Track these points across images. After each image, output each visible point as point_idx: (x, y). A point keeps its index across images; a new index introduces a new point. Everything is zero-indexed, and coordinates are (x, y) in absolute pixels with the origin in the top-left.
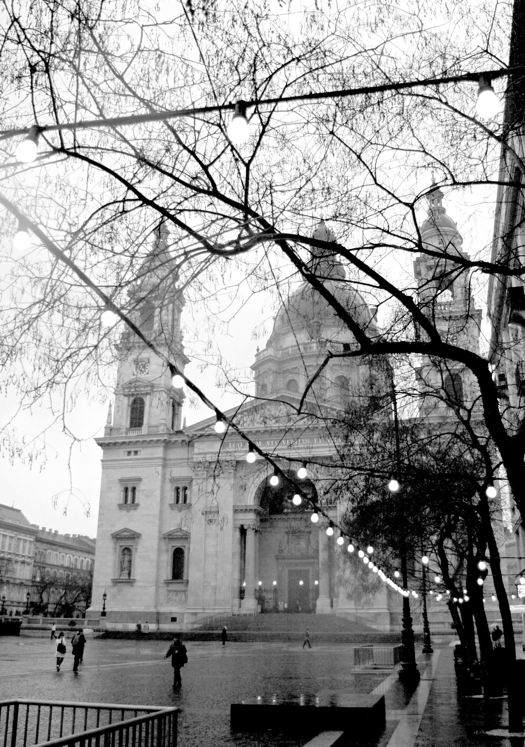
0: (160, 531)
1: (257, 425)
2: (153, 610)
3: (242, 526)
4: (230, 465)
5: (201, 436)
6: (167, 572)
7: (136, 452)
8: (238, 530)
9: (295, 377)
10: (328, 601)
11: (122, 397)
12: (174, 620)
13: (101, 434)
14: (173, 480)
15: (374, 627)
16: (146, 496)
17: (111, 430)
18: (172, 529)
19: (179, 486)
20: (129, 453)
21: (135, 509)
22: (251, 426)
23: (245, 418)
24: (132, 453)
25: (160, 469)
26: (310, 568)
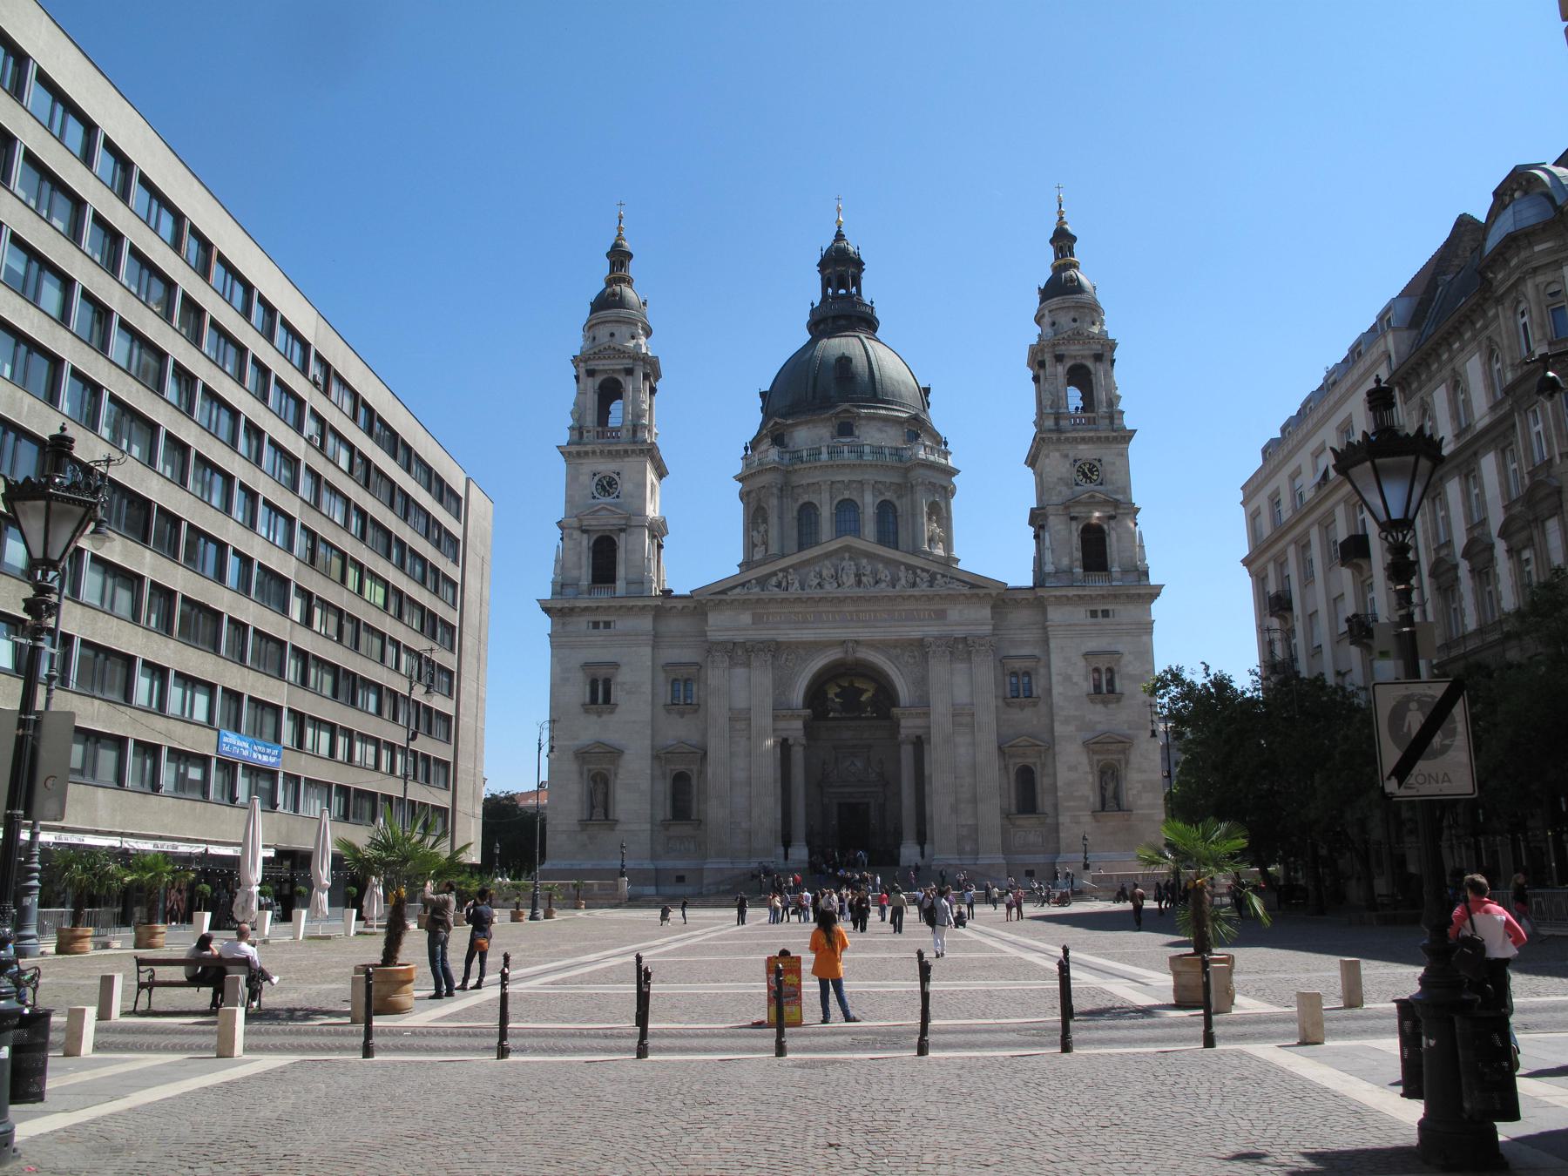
0: (653, 749)
2: (647, 865)
5: (720, 601)
6: (664, 811)
7: (607, 625)
10: (918, 848)
11: (576, 534)
12: (680, 879)
14: (669, 666)
17: (562, 586)
18: (669, 742)
20: (596, 625)
21: (612, 712)
23: (789, 578)
24: (602, 625)
25: (648, 650)
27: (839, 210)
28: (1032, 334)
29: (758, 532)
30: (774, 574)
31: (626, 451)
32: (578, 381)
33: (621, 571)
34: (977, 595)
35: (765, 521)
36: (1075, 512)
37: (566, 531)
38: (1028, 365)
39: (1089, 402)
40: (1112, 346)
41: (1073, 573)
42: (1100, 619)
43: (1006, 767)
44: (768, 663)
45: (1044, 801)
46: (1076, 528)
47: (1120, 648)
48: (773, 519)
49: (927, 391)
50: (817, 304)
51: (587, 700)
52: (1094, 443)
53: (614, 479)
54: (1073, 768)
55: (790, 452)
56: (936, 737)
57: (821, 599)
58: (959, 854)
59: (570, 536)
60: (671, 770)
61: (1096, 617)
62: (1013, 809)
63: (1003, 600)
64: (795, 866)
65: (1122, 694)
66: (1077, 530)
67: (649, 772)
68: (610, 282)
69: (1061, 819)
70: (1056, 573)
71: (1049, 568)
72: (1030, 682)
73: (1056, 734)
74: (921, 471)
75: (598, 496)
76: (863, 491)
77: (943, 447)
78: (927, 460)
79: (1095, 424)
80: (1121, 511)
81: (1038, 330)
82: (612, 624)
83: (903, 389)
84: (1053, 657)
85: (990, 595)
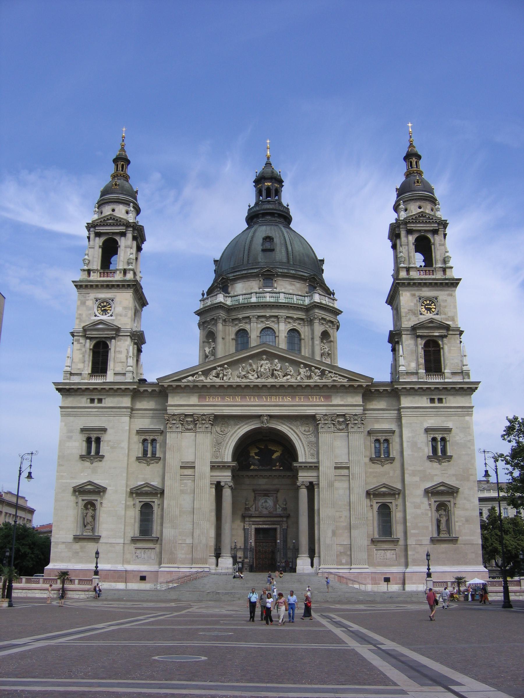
0: (127, 486)
1: (238, 380)
2: (120, 567)
3: (218, 483)
4: (207, 419)
6: (134, 530)
7: (100, 401)
8: (214, 486)
9: (247, 327)
10: (309, 560)
11: (82, 340)
12: (143, 578)
13: (61, 379)
15: (356, 586)
16: (113, 448)
19: (147, 437)
20: (92, 401)
21: (101, 461)
22: (231, 380)
24: (96, 401)
25: (127, 418)
26: (278, 526)
27: (268, 148)
28: (392, 217)
29: (209, 349)
30: (215, 368)
31: (118, 286)
32: (89, 241)
33: (111, 365)
34: (352, 386)
35: (214, 340)
36: (420, 332)
37: (75, 338)
38: (389, 238)
39: (429, 261)
40: (445, 224)
41: (417, 373)
42: (437, 404)
43: (371, 506)
44: (208, 429)
45: (398, 531)
46: (421, 342)
47: (450, 425)
48: (219, 340)
49: (322, 261)
50: (252, 205)
51: (84, 453)
52: (433, 287)
53: (109, 304)
54: (417, 506)
55: (231, 297)
56: (323, 483)
57: (247, 387)
58: (337, 565)
59: (78, 341)
60: (140, 502)
61: (434, 403)
62: (376, 536)
63: (370, 390)
64: (223, 571)
65: (451, 457)
66: (421, 344)
67: (124, 502)
68: (114, 176)
69: (409, 542)
70: (406, 373)
71: (402, 368)
72: (388, 447)
73: (406, 483)
74: (316, 311)
75: (98, 315)
76: (279, 323)
77: (332, 296)
78: (321, 303)
79: (433, 275)
80: (451, 333)
81: (395, 215)
82: (103, 400)
83: (306, 259)
84: (404, 429)
85: (361, 386)
